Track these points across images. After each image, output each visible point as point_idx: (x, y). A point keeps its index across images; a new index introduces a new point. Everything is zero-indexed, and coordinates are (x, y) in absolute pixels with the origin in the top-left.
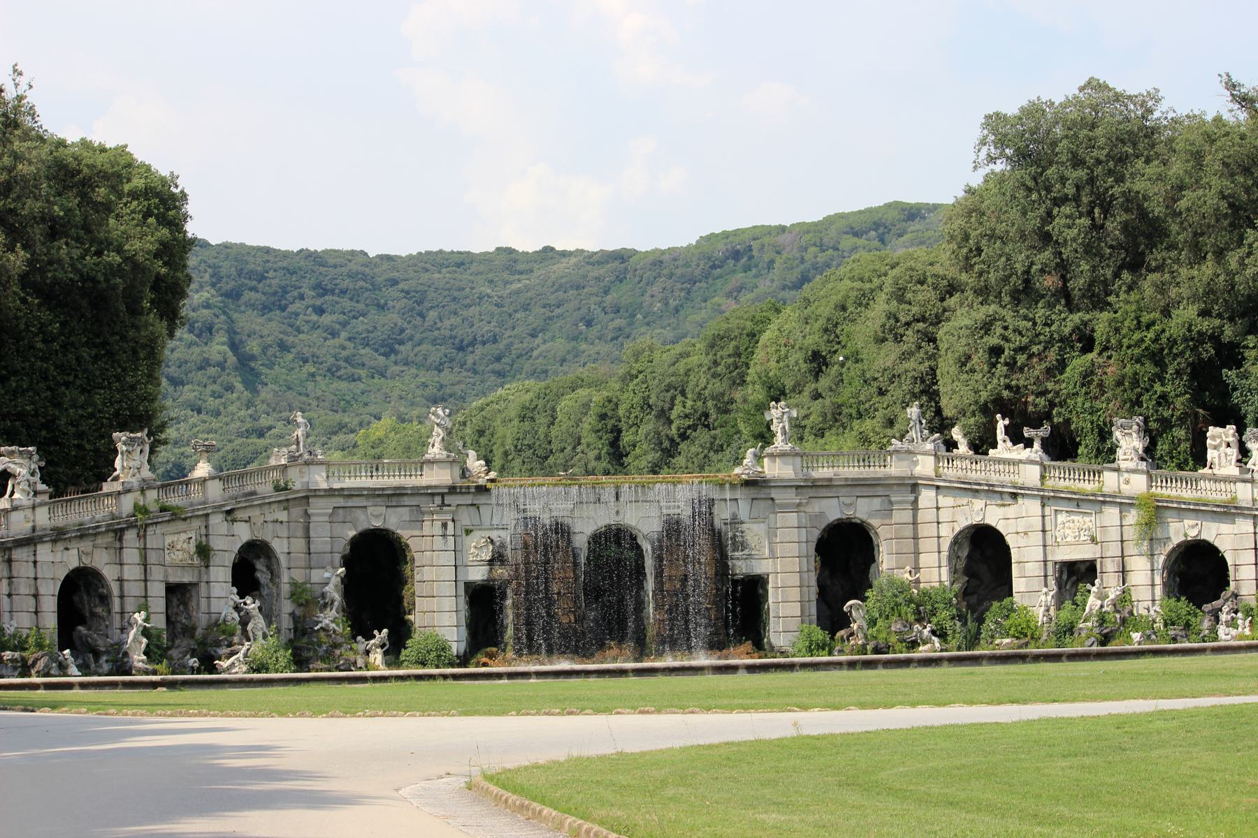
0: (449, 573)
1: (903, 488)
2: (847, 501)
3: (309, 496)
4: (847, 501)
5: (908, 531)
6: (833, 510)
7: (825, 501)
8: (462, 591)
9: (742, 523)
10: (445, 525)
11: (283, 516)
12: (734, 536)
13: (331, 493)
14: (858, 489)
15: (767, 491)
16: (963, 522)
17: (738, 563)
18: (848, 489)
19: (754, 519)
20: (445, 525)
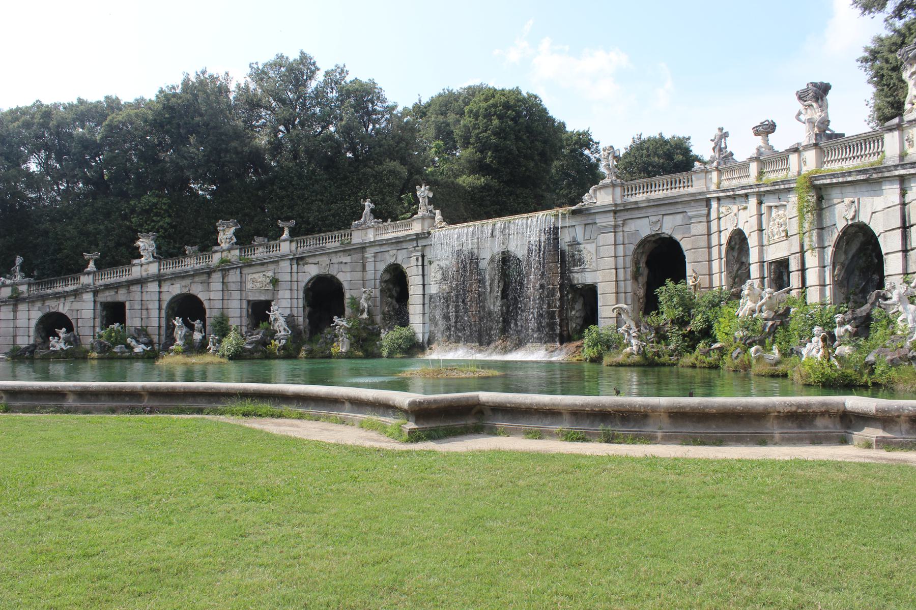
0: (419, 290)
1: (699, 204)
2: (653, 219)
3: (363, 248)
4: (653, 219)
5: (703, 242)
6: (643, 228)
7: (639, 221)
8: (427, 301)
9: (579, 244)
10: (417, 259)
11: (347, 259)
12: (573, 256)
13: (373, 244)
14: (662, 208)
15: (593, 217)
16: (731, 228)
17: (576, 275)
18: (655, 209)
19: (589, 240)
20: (417, 259)
